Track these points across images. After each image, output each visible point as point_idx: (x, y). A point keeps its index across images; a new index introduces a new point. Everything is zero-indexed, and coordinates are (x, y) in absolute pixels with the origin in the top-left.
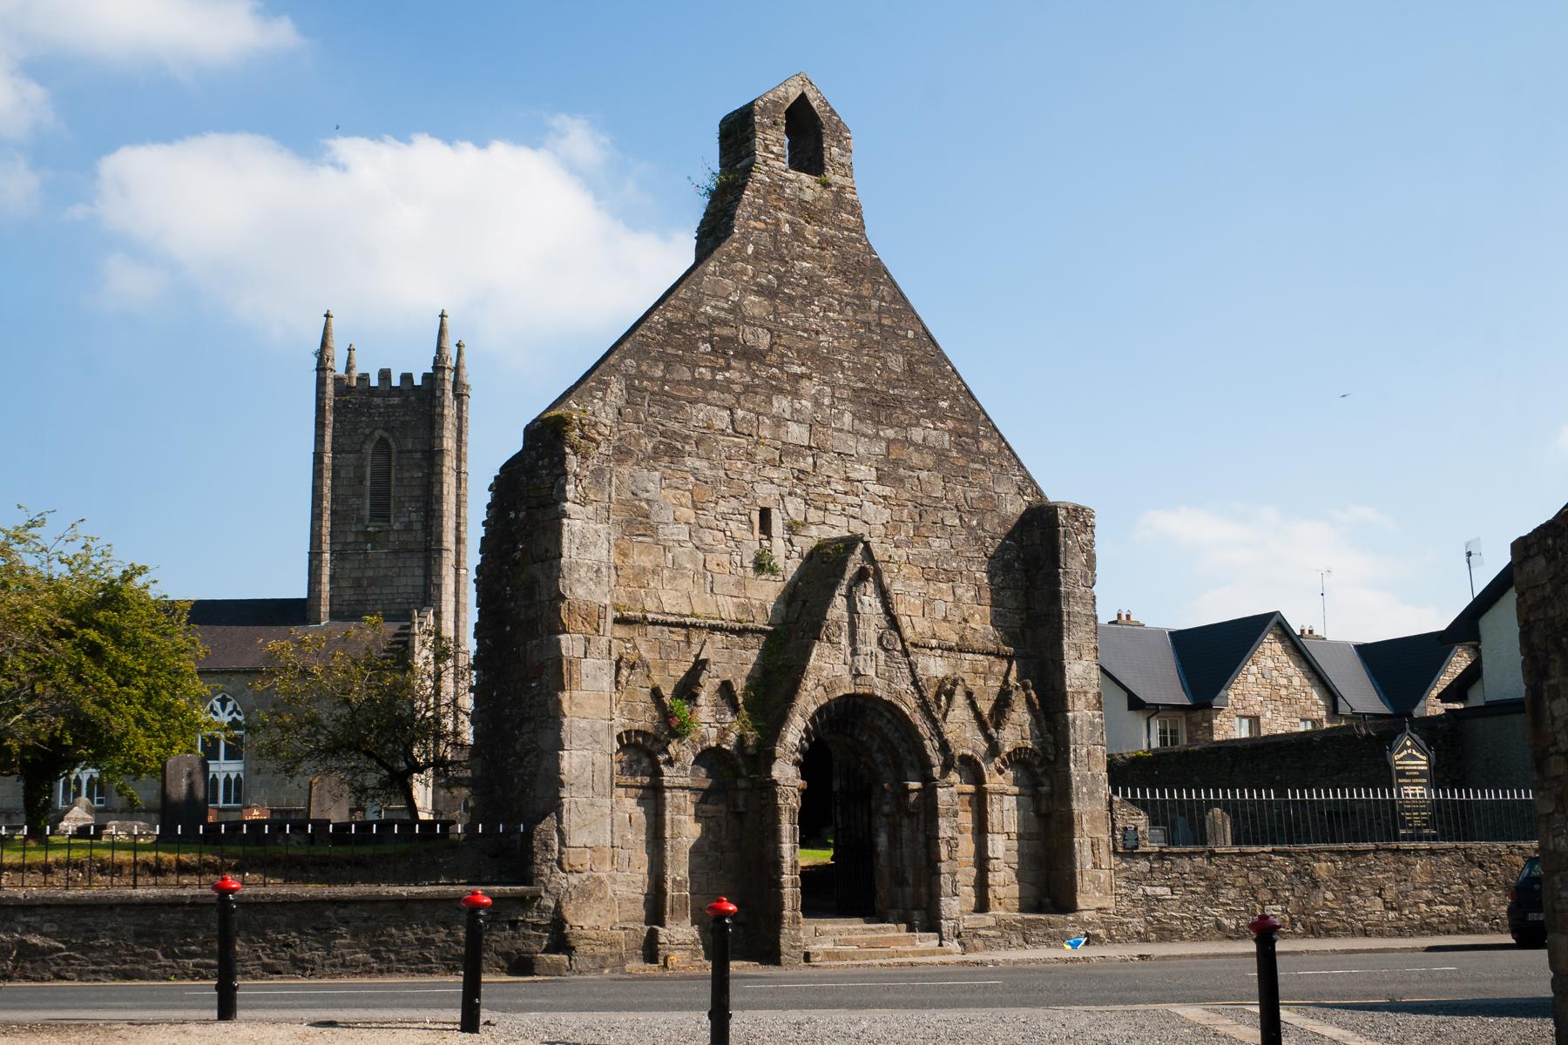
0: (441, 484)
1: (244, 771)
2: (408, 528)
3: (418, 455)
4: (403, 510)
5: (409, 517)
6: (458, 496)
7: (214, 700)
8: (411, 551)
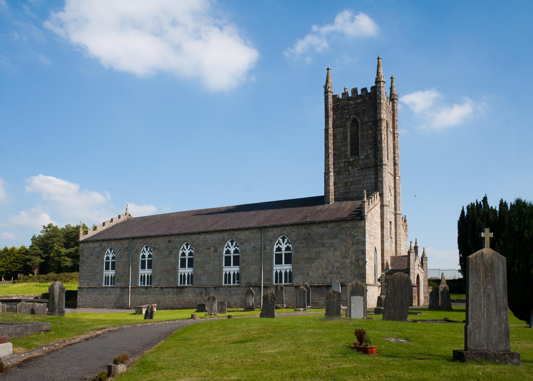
0: (381, 134)
1: (292, 269)
2: (367, 157)
3: (371, 124)
4: (365, 149)
5: (367, 152)
6: (394, 144)
7: (279, 238)
8: (369, 167)
